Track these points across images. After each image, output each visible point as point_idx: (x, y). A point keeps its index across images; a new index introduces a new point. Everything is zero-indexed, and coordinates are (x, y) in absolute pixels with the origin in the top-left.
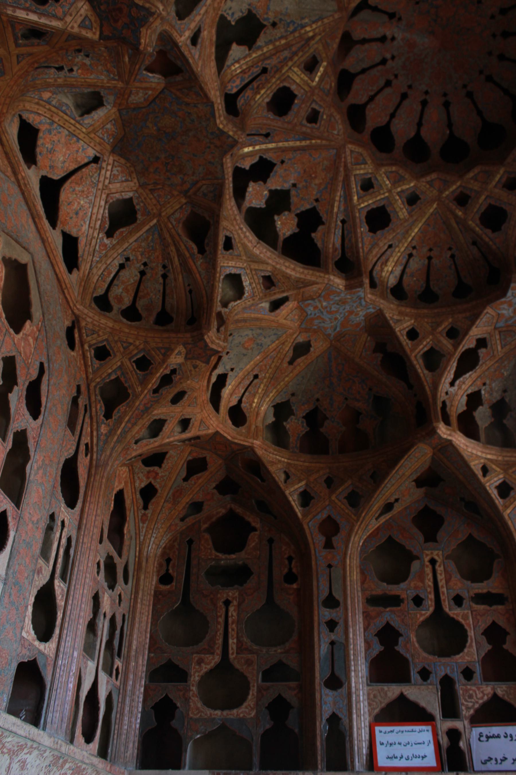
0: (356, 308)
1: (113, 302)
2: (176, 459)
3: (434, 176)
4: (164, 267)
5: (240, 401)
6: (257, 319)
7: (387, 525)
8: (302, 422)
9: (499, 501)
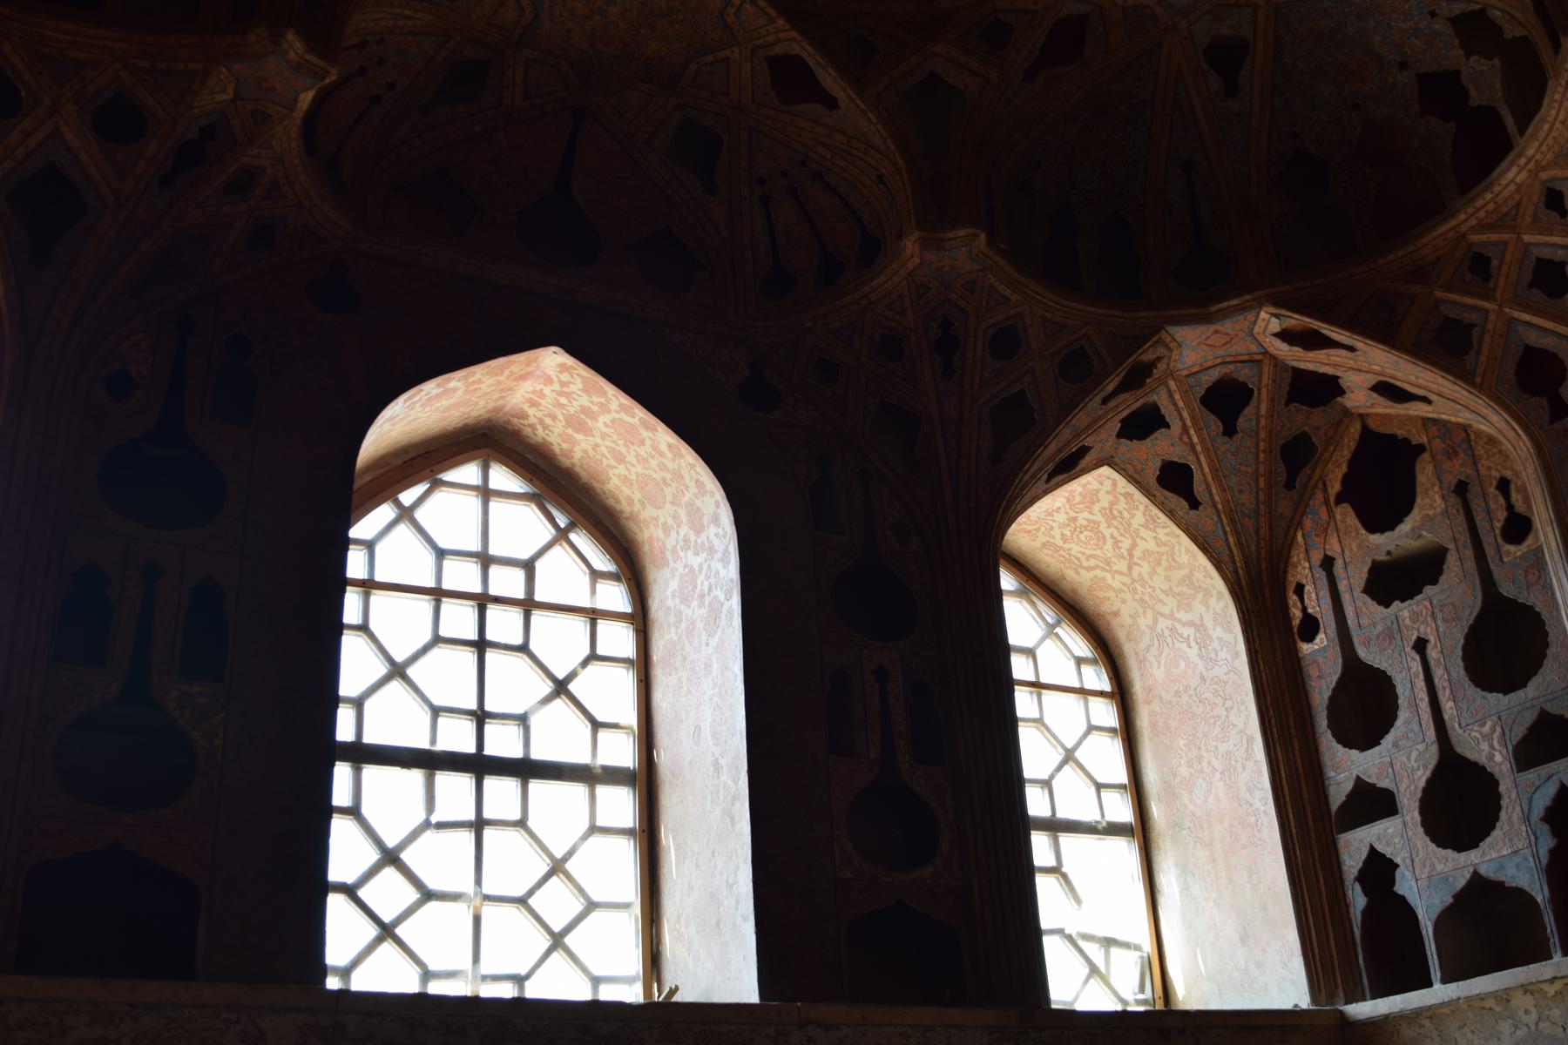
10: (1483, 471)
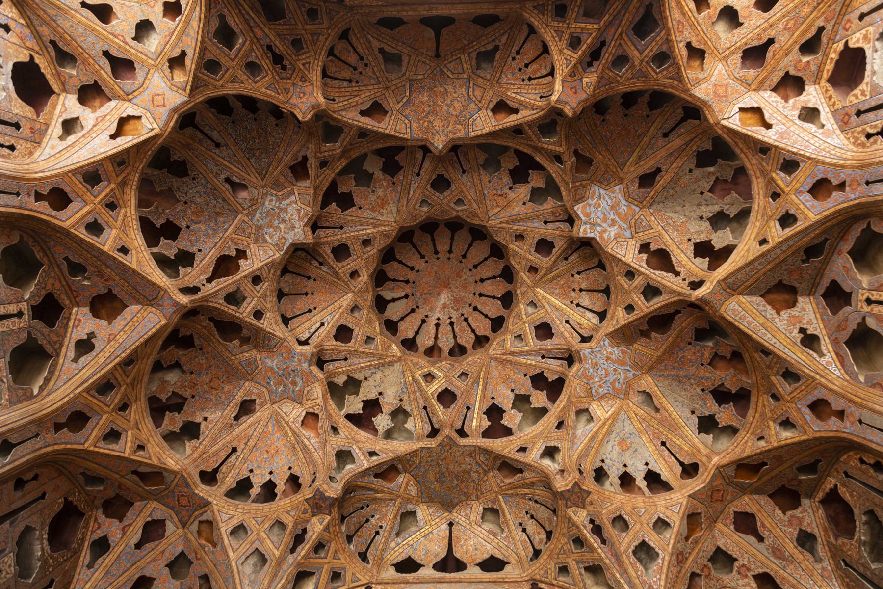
1: (538, 548)
2: (729, 541)
3: (518, 291)
4: (530, 499)
5: (682, 464)
6: (593, 438)
7: (835, 342)
8: (724, 408)
9: (799, 226)
10: (21, 141)
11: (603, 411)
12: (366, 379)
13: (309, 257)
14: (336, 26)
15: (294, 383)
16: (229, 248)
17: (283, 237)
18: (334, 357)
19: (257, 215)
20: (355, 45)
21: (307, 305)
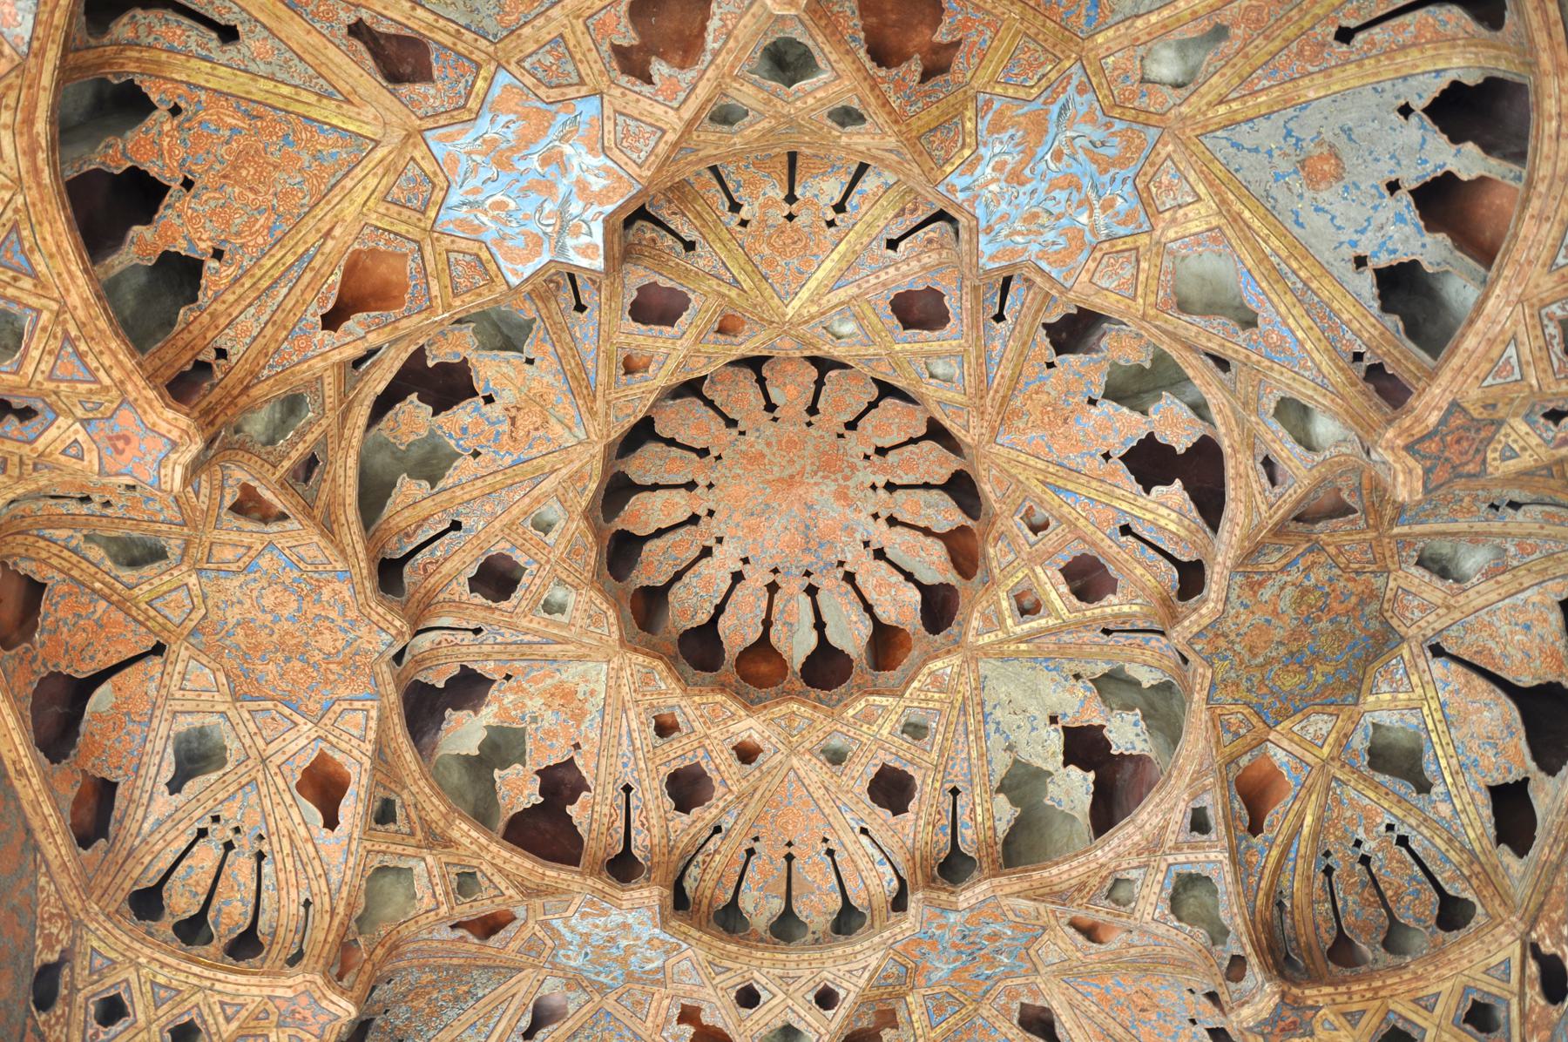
0: (1002, 194)
11: (1191, 211)
12: (1010, 748)
13: (700, 858)
14: (129, 948)
15: (994, 937)
16: (677, 1037)
17: (648, 942)
18: (947, 821)
19: (602, 978)
20: (171, 859)
21: (817, 859)
